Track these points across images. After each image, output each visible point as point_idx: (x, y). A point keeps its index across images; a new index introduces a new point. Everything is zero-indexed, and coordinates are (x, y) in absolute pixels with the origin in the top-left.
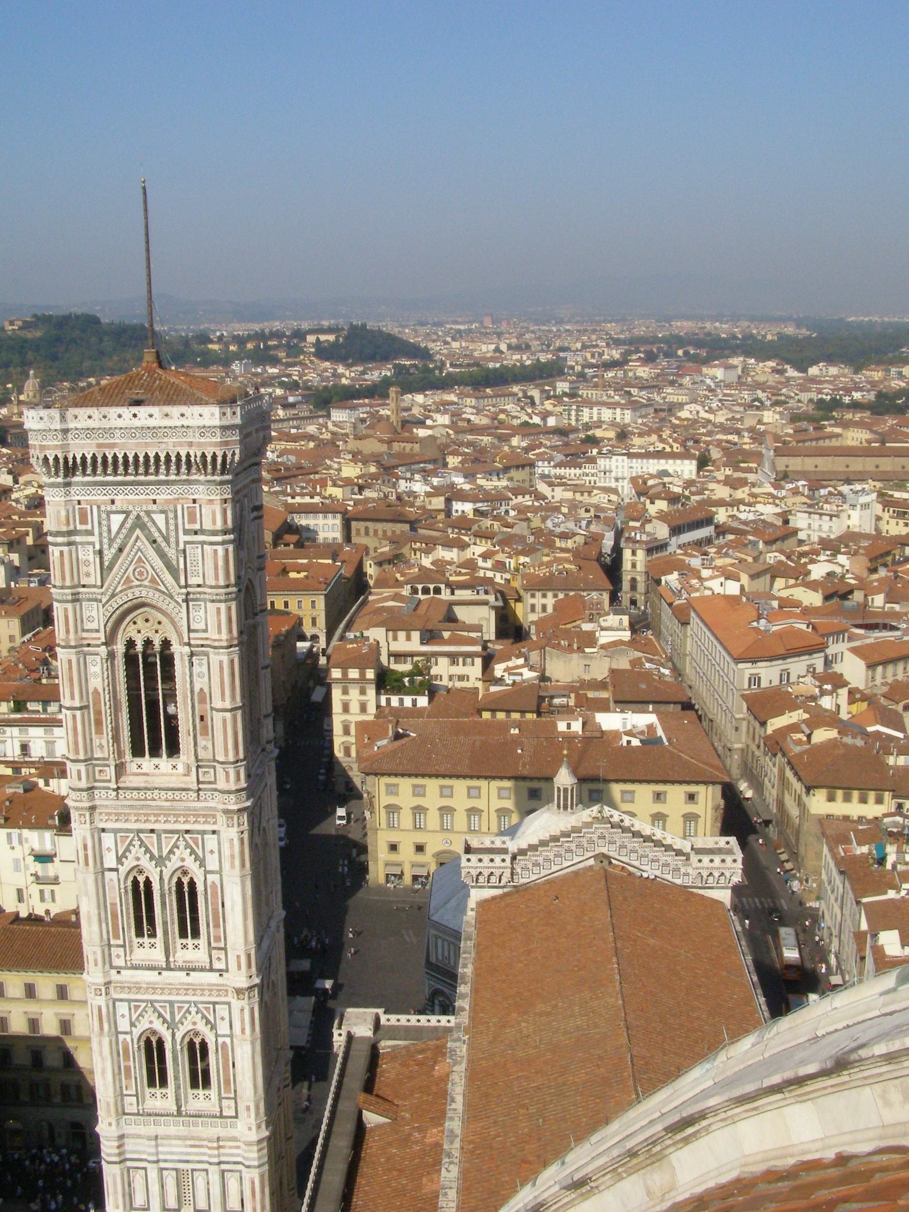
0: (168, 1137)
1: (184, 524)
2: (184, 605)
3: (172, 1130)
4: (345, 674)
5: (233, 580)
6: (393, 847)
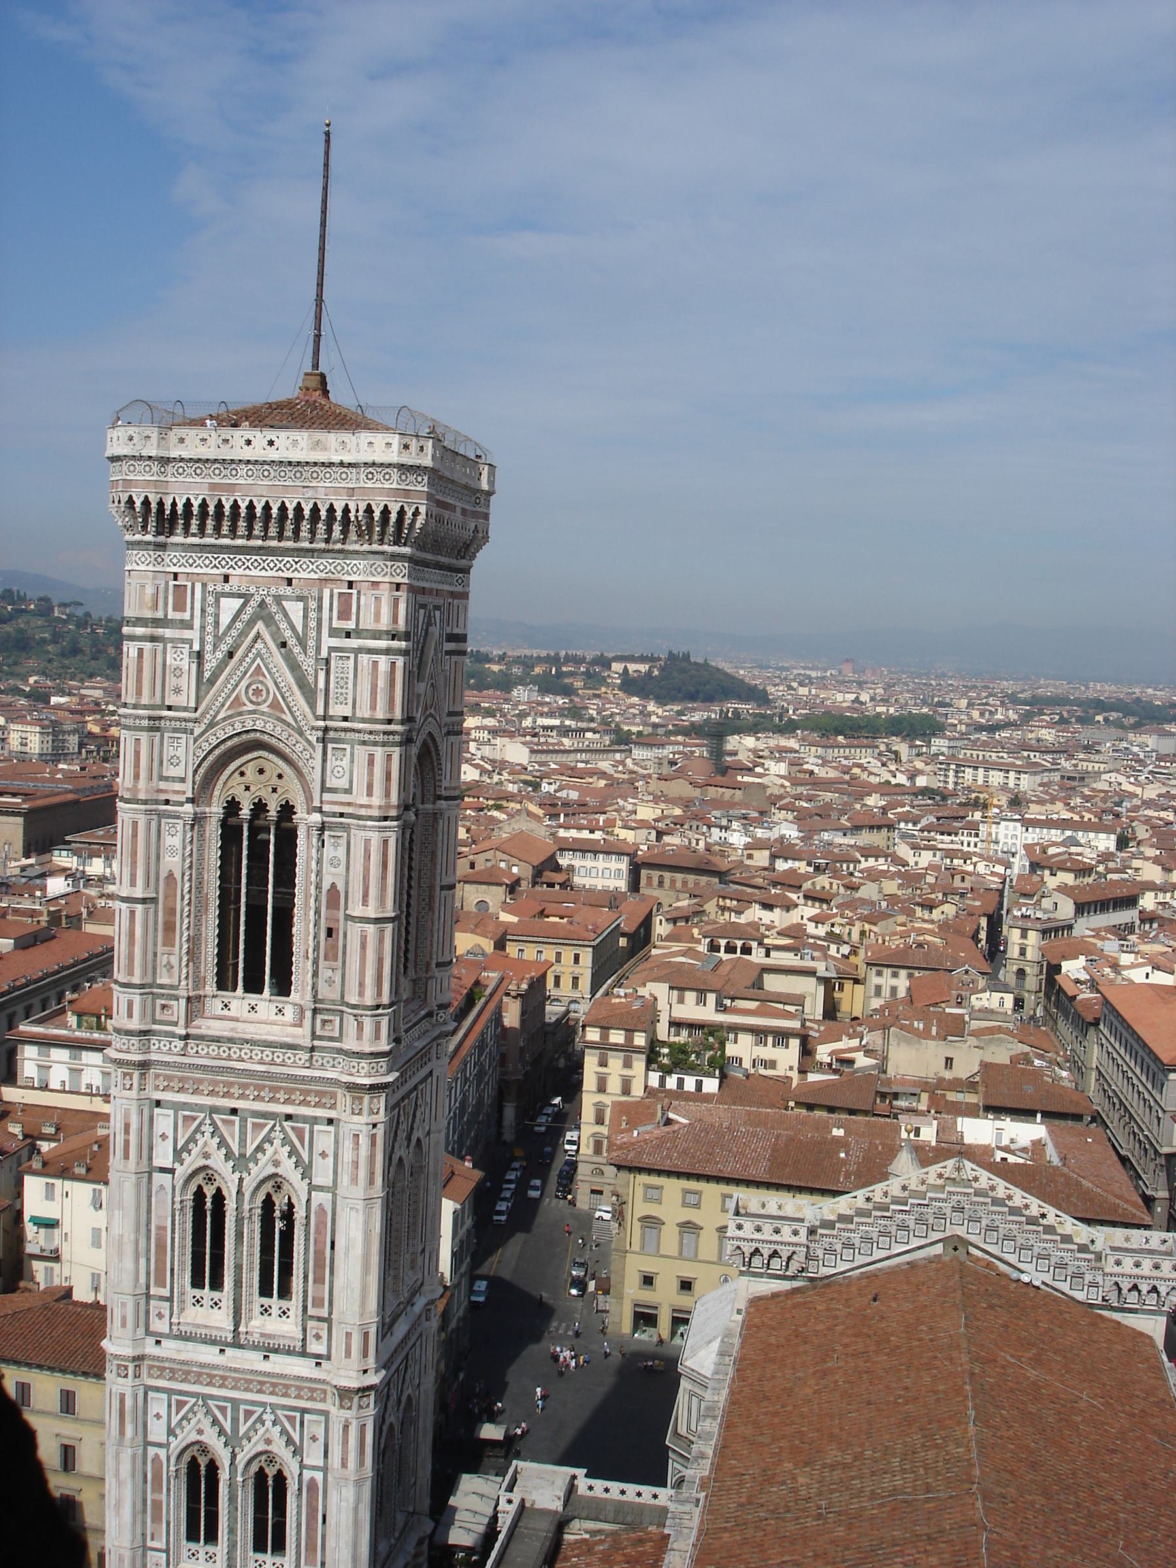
1: (331, 619)
4: (605, 1036)
5: (398, 714)
6: (648, 1280)
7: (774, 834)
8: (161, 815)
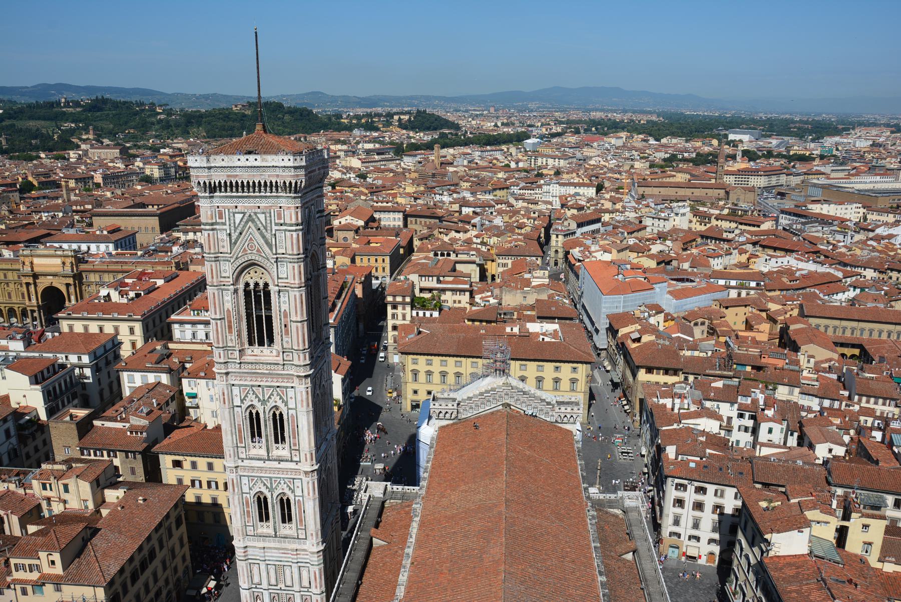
0: (270, 548)
2: (275, 264)
3: (272, 545)
4: (394, 299)
5: (301, 251)
6: (415, 392)
7: (461, 196)
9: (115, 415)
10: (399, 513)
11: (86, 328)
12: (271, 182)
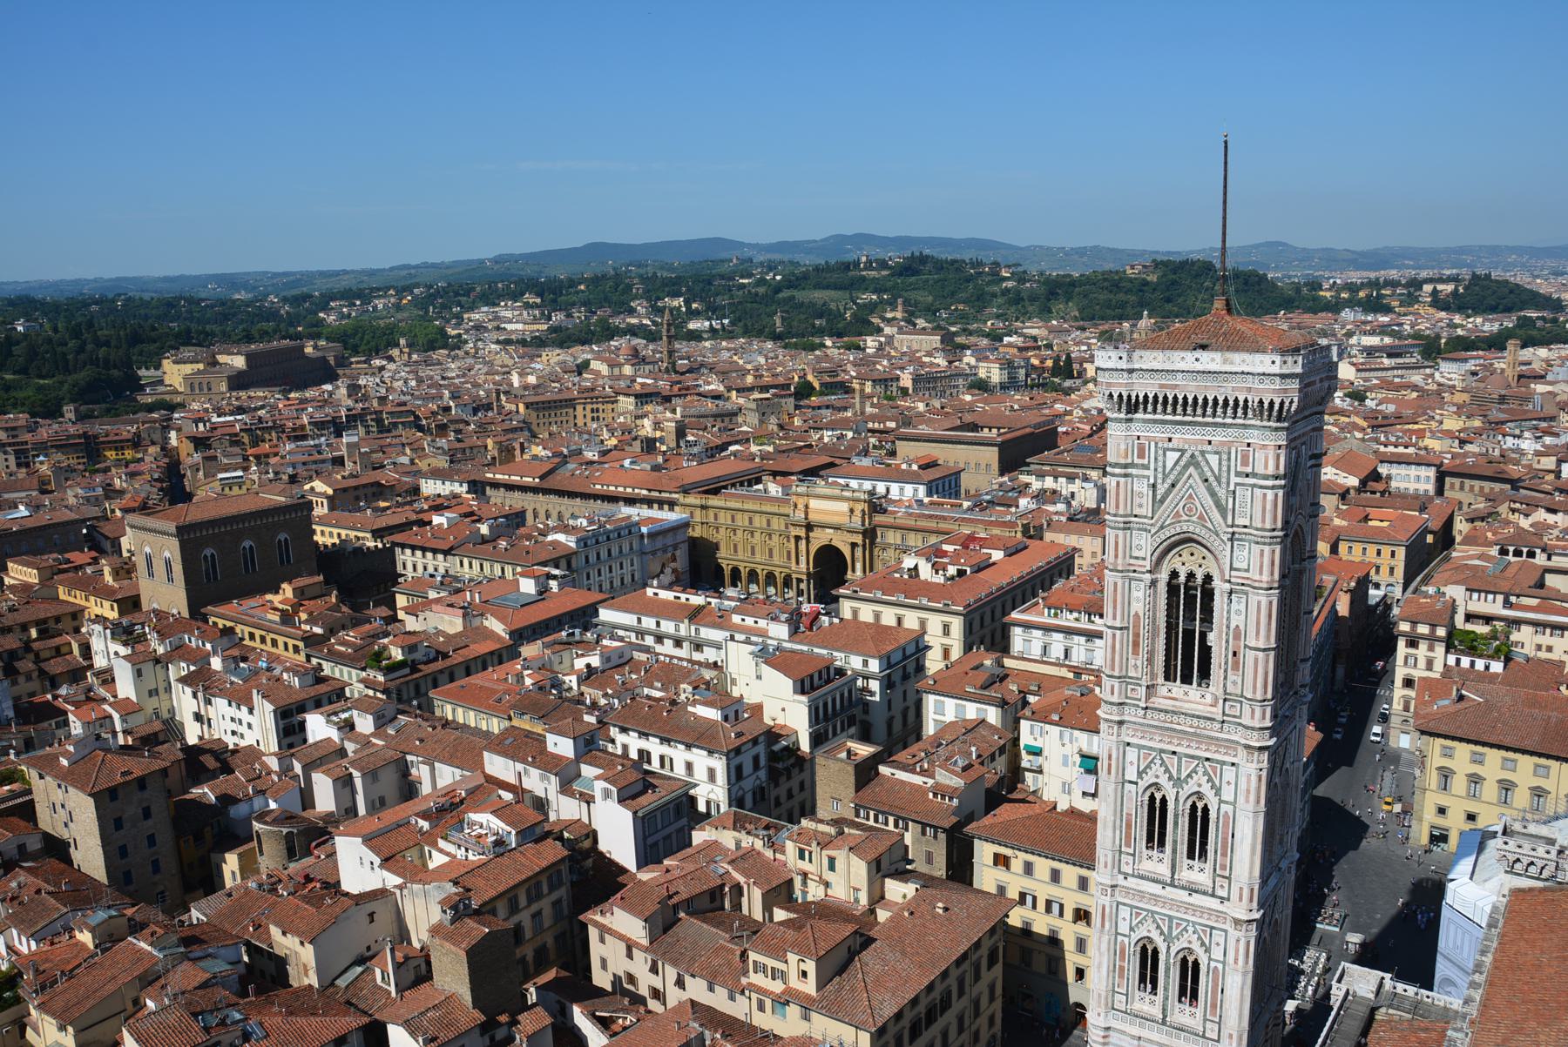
2: (1229, 544)
3: (1155, 1036)
5: (1279, 525)
8: (1131, 579)
9: (911, 762)
10: (1403, 1038)
11: (877, 616)
12: (1236, 400)
